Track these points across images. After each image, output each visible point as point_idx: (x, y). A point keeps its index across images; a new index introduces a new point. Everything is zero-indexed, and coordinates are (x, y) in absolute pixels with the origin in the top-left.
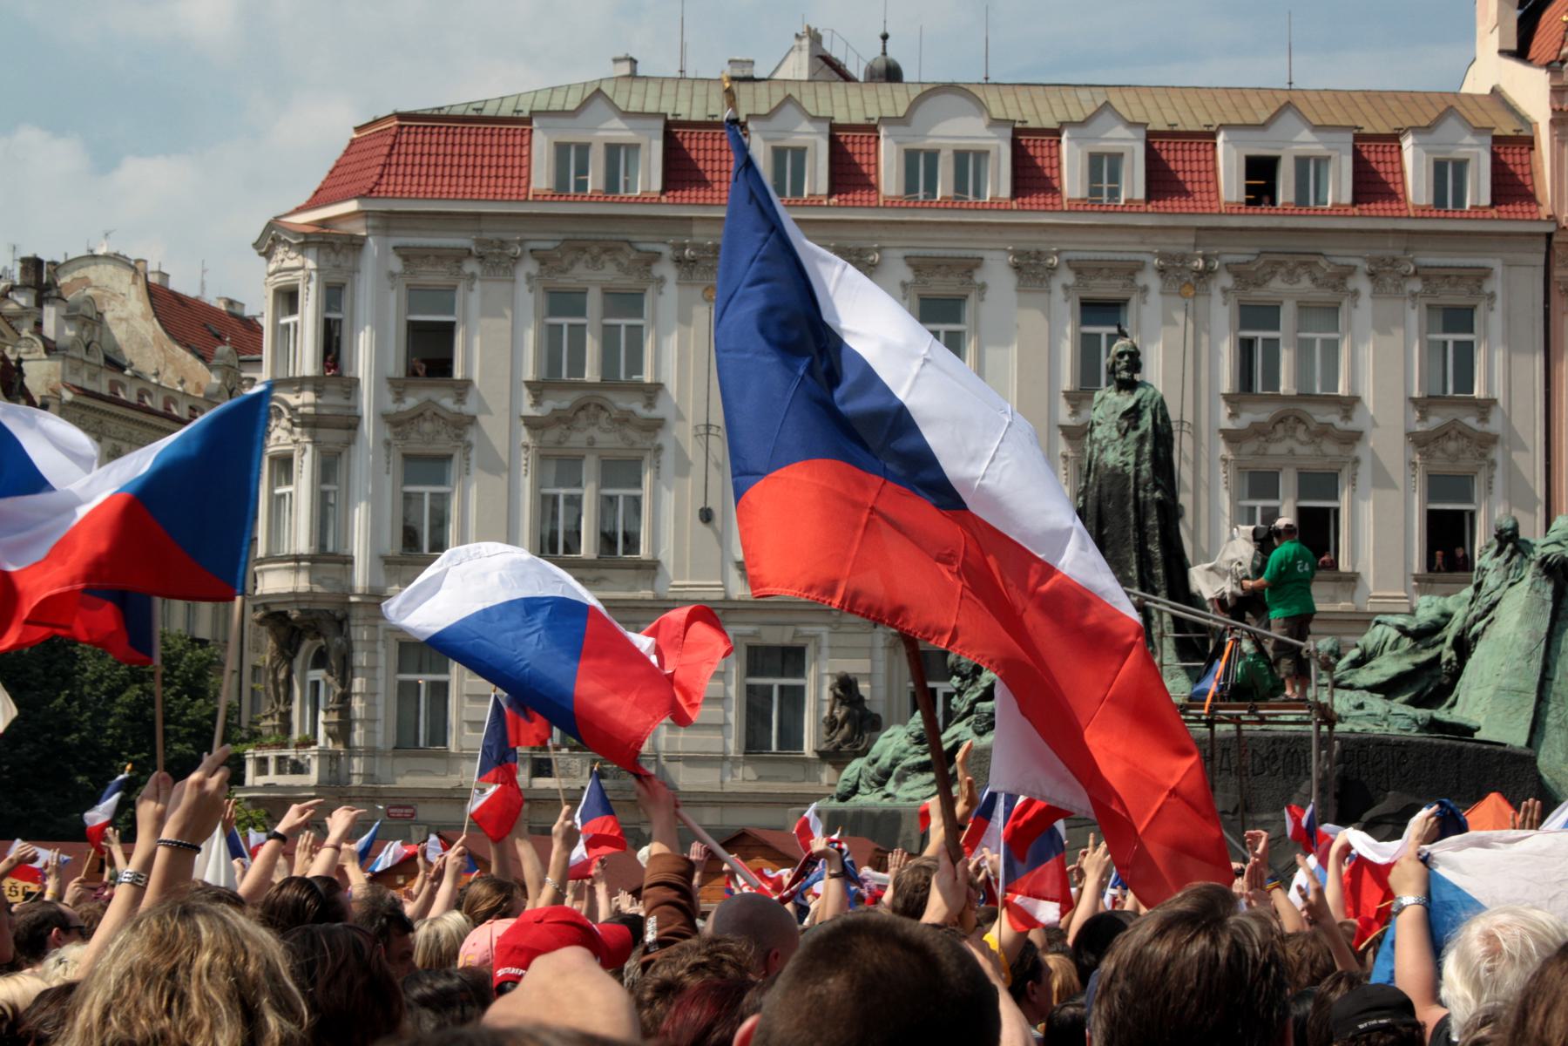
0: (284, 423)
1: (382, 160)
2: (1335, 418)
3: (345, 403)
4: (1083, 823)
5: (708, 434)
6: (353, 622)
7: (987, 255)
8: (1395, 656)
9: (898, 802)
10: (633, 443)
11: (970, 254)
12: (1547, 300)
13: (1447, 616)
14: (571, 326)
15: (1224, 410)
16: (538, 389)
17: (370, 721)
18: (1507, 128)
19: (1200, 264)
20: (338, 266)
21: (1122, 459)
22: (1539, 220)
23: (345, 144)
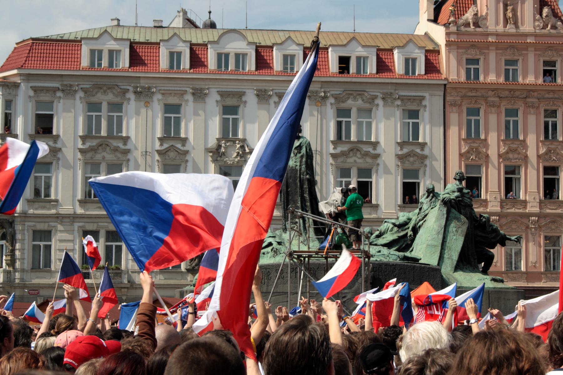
1: (26, 55)
2: (370, 149)
4: (281, 294)
5: (146, 155)
6: (16, 223)
7: (247, 91)
8: (391, 234)
10: (119, 158)
11: (241, 90)
13: (410, 219)
14: (96, 116)
15: (331, 147)
16: (84, 138)
17: (22, 259)
18: (430, 47)
19: (323, 94)
20: (10, 94)
21: (295, 164)
22: (442, 79)
23: (12, 49)
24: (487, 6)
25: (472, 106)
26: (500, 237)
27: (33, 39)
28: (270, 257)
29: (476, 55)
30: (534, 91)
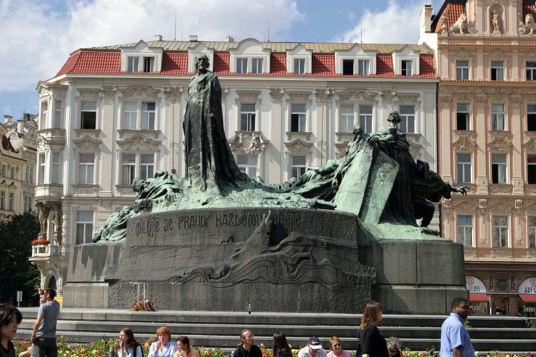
0: (43, 143)
3: (61, 137)
4: (170, 247)
6: (63, 205)
8: (313, 182)
9: (110, 242)
10: (151, 149)
12: (437, 103)
13: (336, 166)
15: (336, 138)
16: (122, 132)
17: (67, 236)
18: (425, 52)
22: (435, 78)
23: (68, 59)
24: (475, 14)
25: (461, 102)
26: (442, 187)
27: (82, 50)
28: (163, 206)
29: (465, 57)
30: (517, 88)
